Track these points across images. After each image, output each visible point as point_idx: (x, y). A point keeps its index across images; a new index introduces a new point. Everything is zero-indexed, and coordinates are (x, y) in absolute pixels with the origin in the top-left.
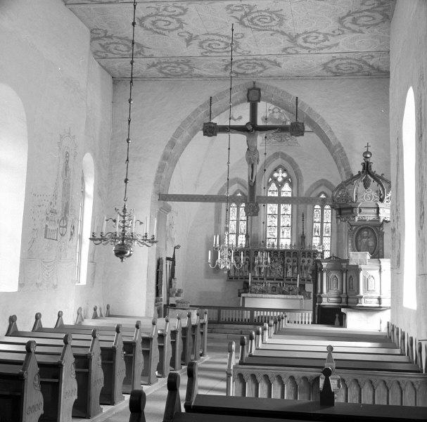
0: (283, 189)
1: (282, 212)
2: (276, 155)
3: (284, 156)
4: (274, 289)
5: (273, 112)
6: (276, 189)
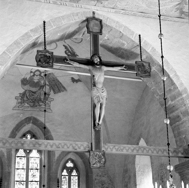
0: (31, 155)
2: (28, 120)
3: (35, 121)
5: (34, 75)
6: (24, 154)
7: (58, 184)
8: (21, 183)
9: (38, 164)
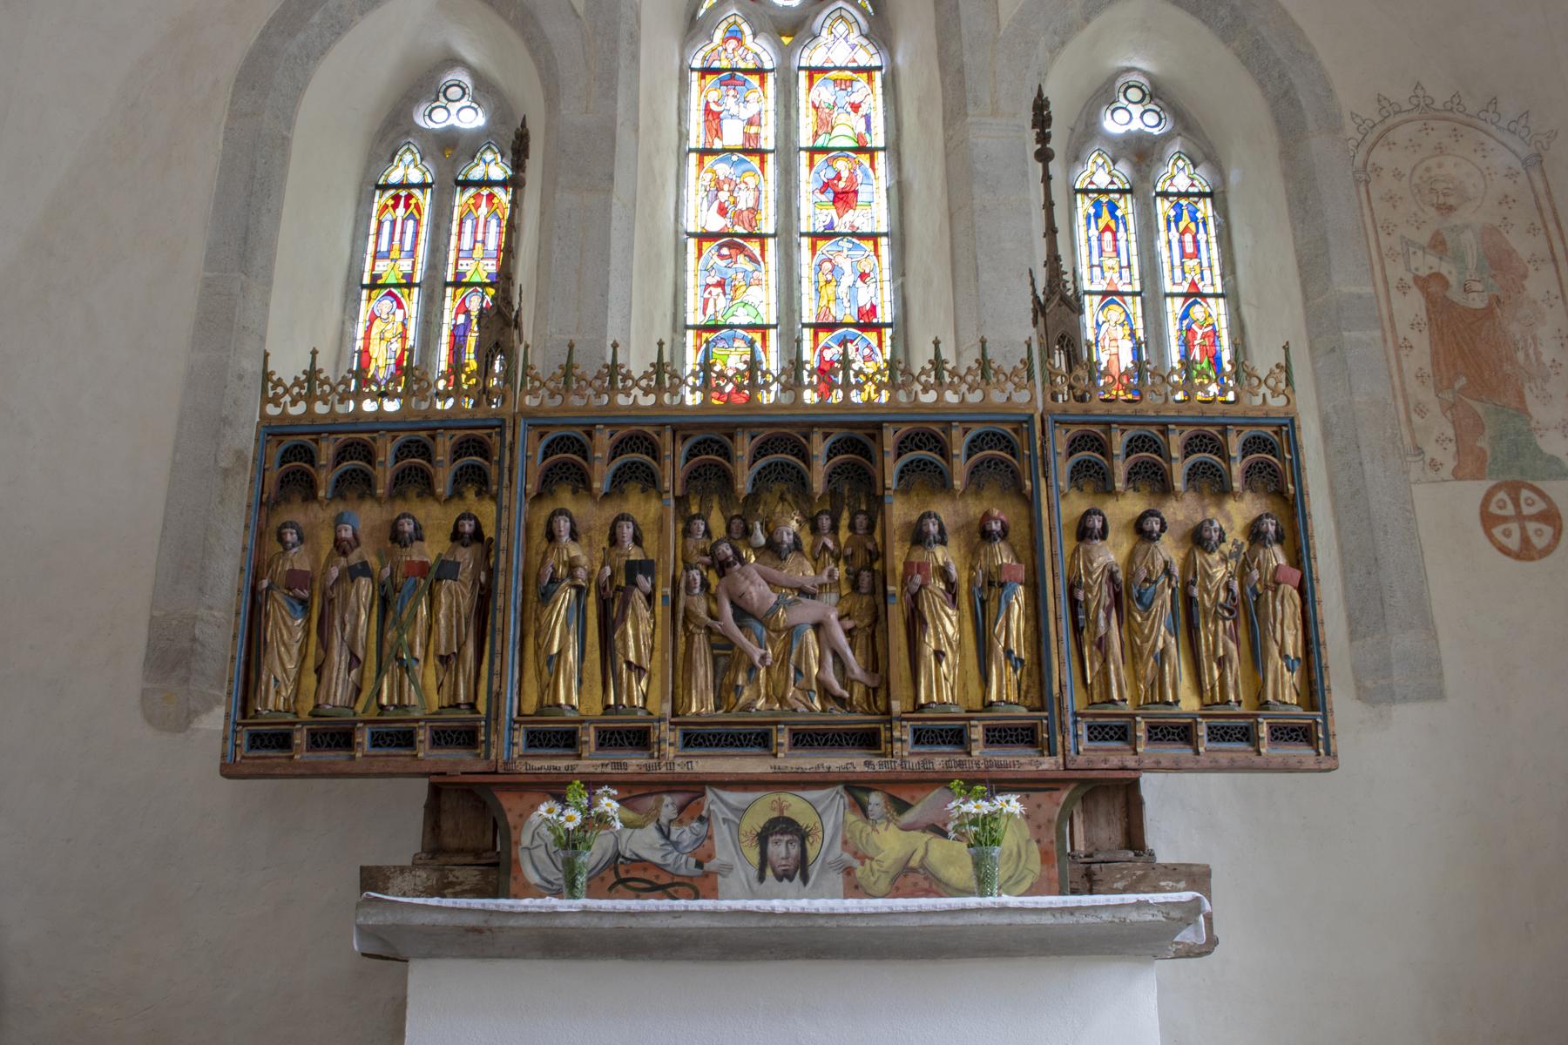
0: (814, 56)
1: (814, 211)
4: (780, 849)
7: (1043, 138)
8: (741, 249)
9: (867, 118)
